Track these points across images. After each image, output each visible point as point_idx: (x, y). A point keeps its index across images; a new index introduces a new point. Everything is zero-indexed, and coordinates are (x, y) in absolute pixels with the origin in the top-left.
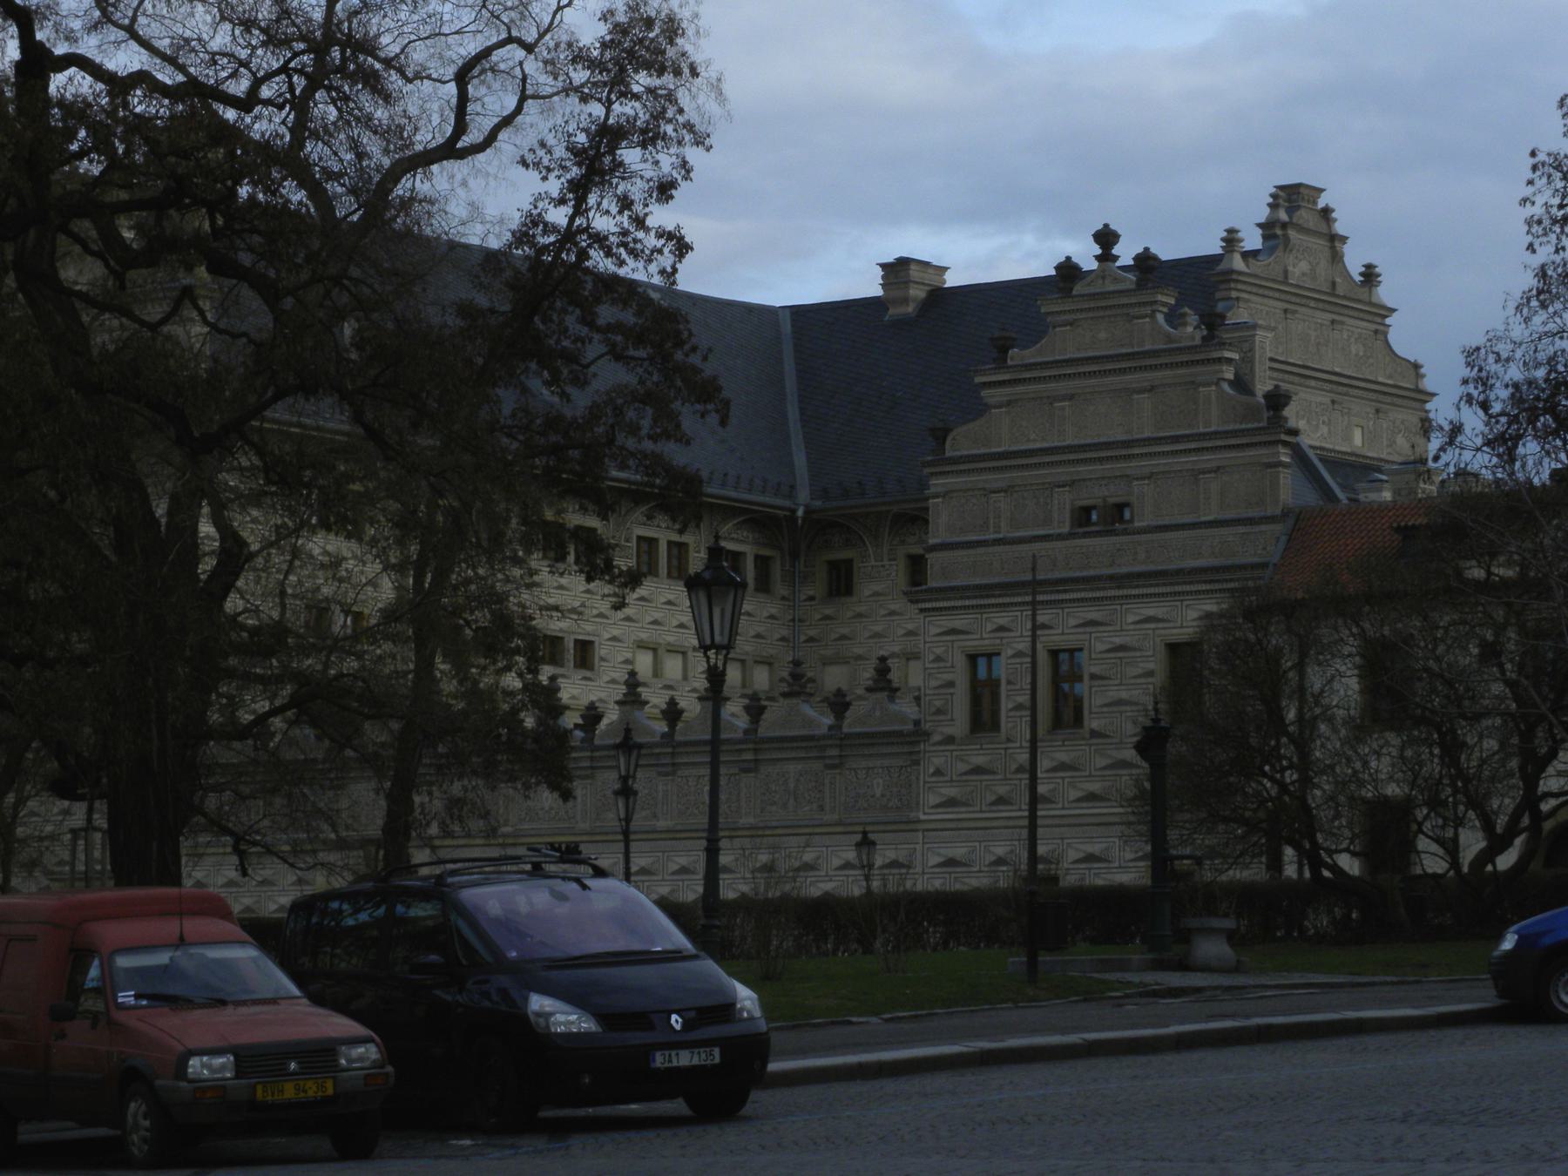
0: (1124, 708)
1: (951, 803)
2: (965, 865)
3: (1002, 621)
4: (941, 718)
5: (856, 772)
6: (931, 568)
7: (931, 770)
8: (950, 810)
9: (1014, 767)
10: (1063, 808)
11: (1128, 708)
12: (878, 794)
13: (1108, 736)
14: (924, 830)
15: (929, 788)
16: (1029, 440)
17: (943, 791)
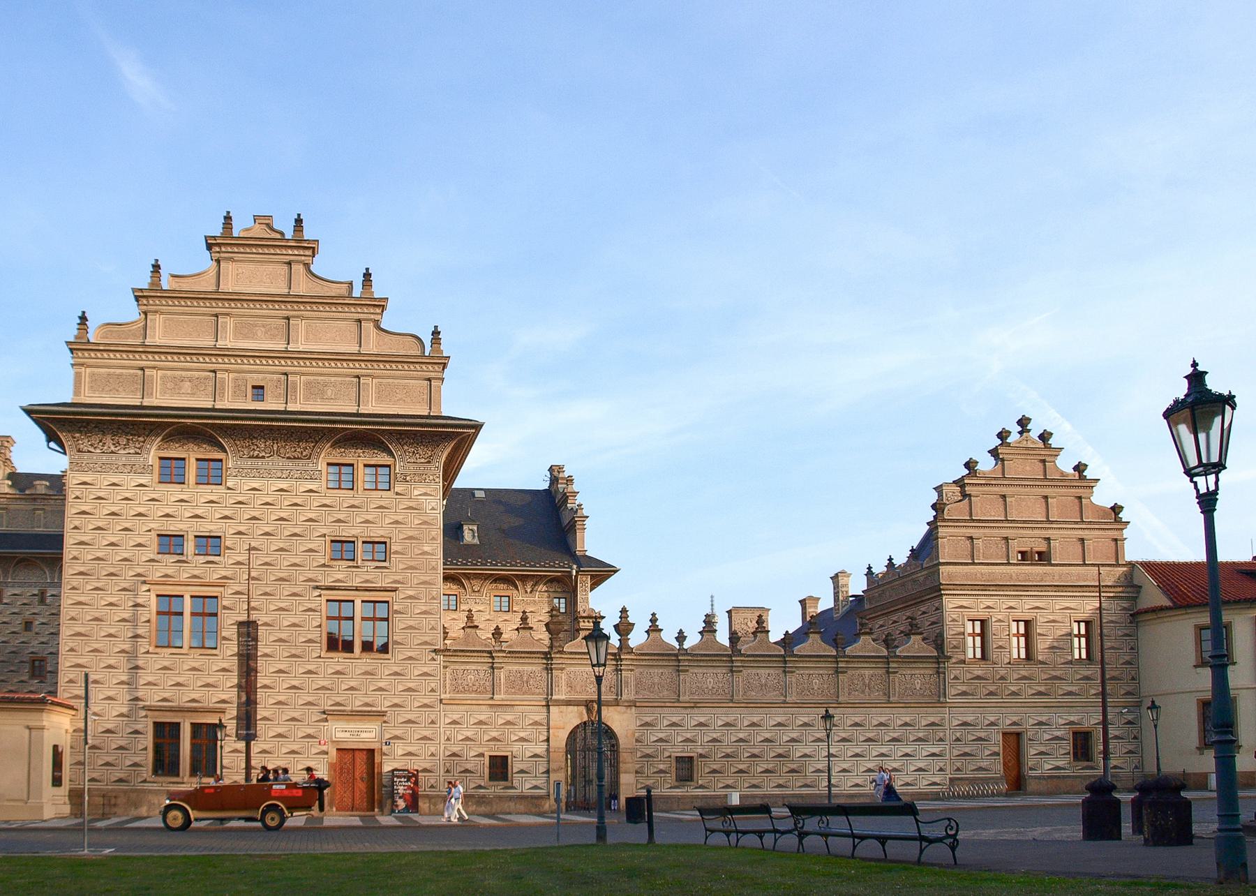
0: (1055, 651)
1: (964, 693)
2: (972, 725)
3: (989, 604)
4: (957, 650)
5: (905, 677)
6: (942, 574)
7: (952, 677)
8: (964, 697)
9: (998, 677)
10: (1025, 699)
11: (1058, 651)
12: (918, 688)
13: (1047, 664)
14: (949, 707)
15: (951, 686)
16: (991, 515)
17: (959, 687)
